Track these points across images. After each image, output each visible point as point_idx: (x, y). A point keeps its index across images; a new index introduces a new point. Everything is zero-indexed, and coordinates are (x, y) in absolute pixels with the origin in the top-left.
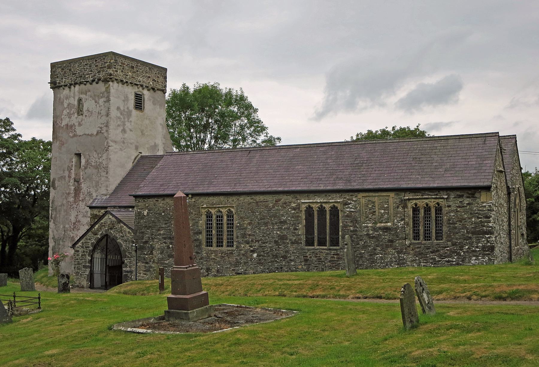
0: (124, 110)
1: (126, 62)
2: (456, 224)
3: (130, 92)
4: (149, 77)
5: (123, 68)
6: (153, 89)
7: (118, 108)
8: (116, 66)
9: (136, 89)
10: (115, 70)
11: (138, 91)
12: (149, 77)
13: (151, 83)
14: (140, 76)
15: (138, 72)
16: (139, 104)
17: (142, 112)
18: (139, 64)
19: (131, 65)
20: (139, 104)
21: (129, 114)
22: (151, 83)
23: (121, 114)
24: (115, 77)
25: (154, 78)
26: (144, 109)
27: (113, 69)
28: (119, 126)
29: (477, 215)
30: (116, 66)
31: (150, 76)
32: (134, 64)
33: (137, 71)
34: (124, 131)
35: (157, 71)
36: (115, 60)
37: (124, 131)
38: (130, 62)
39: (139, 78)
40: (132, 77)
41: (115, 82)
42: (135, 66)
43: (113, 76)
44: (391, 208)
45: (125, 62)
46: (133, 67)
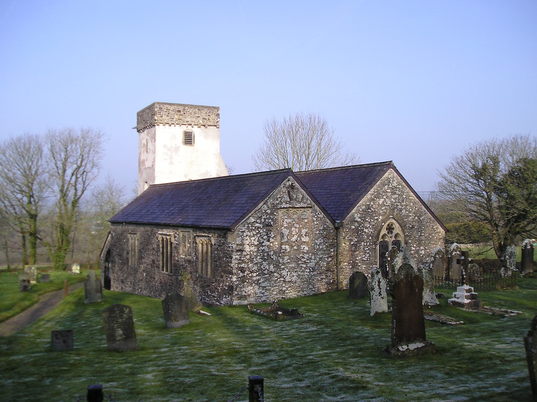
0: (171, 147)
1: (172, 108)
2: (217, 262)
3: (178, 132)
4: (199, 117)
5: (169, 114)
6: (204, 126)
7: (165, 146)
8: (160, 112)
9: (185, 128)
10: (159, 116)
11: (187, 130)
12: (199, 117)
13: (201, 122)
14: (188, 117)
15: (186, 114)
16: (189, 139)
17: (192, 146)
18: (187, 108)
19: (177, 109)
20: (189, 139)
21: (177, 149)
22: (201, 122)
23: (168, 150)
24: (160, 122)
25: (205, 117)
26: (194, 144)
27: (158, 115)
28: (165, 160)
29: (226, 255)
30: (160, 112)
31: (200, 116)
32: (181, 109)
33: (184, 114)
34: (171, 163)
35: (208, 111)
36: (159, 108)
37: (171, 163)
38: (176, 107)
39: (186, 119)
40: (179, 119)
41: (161, 125)
42: (181, 110)
43: (158, 120)
44: (191, 243)
45: (170, 108)
46: (180, 111)
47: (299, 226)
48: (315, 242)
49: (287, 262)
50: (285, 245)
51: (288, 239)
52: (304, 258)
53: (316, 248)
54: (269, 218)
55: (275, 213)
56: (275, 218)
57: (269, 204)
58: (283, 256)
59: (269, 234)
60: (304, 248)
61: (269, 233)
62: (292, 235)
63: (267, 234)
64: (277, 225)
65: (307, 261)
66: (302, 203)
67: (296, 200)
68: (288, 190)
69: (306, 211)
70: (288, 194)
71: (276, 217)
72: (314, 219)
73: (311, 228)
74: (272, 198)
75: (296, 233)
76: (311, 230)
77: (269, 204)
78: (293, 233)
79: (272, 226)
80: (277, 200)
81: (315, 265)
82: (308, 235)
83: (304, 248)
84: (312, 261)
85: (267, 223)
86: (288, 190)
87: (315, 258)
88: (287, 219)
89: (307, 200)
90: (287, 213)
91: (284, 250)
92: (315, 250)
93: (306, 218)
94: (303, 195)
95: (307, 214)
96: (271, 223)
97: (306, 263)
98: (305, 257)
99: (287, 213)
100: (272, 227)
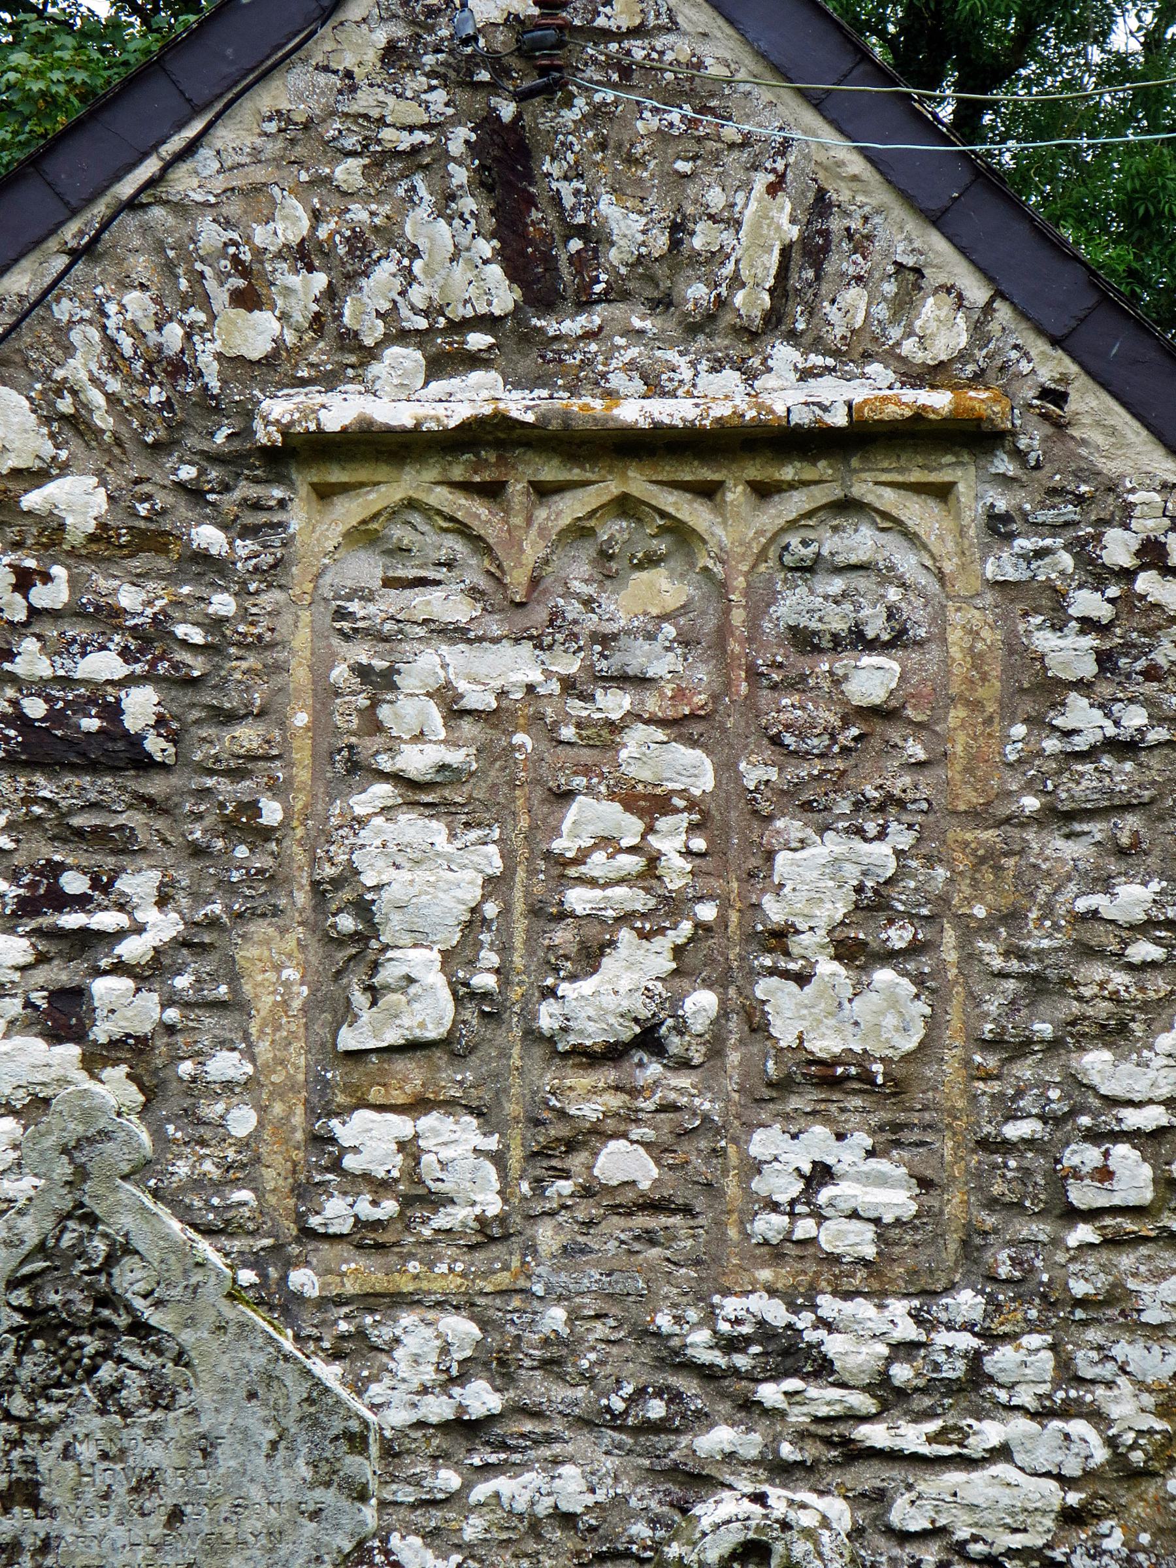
47: (726, 769)
48: (1075, 1083)
49: (438, 1409)
50: (418, 1106)
51: (463, 994)
52: (823, 1369)
53: (1081, 1195)
54: (74, 612)
55: (209, 537)
56: (216, 624)
57: (77, 369)
58: (370, 1301)
59: (81, 902)
60: (821, 1174)
61: (74, 883)
62: (563, 936)
63: (28, 907)
64: (248, 736)
65: (875, 1435)
66: (784, 354)
67: (663, 303)
68: (488, 123)
69: (888, 499)
70: (483, 183)
71: (223, 604)
72: (1045, 641)
73: (977, 816)
74: (141, 266)
75: (635, 899)
76: (988, 859)
77: (77, 369)
78: (579, 899)
79: (145, 764)
80: (247, 300)
81: (1071, 1517)
82: (898, 937)
83: (821, 1174)
84: (990, 1433)
85: (35, 708)
86: (488, 123)
87: (1067, 1373)
88: (455, 634)
89: (903, 305)
90: (463, 530)
91: (380, 1187)
92: (1084, 1233)
93: (876, 627)
94: (821, 205)
95: (907, 562)
96: (113, 712)
97: (867, 1477)
98: (834, 1345)
99: (463, 530)
100: (155, 786)
